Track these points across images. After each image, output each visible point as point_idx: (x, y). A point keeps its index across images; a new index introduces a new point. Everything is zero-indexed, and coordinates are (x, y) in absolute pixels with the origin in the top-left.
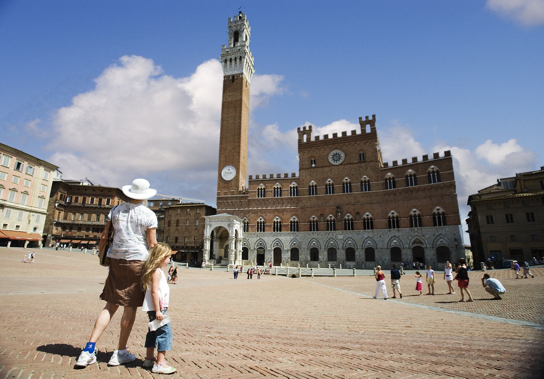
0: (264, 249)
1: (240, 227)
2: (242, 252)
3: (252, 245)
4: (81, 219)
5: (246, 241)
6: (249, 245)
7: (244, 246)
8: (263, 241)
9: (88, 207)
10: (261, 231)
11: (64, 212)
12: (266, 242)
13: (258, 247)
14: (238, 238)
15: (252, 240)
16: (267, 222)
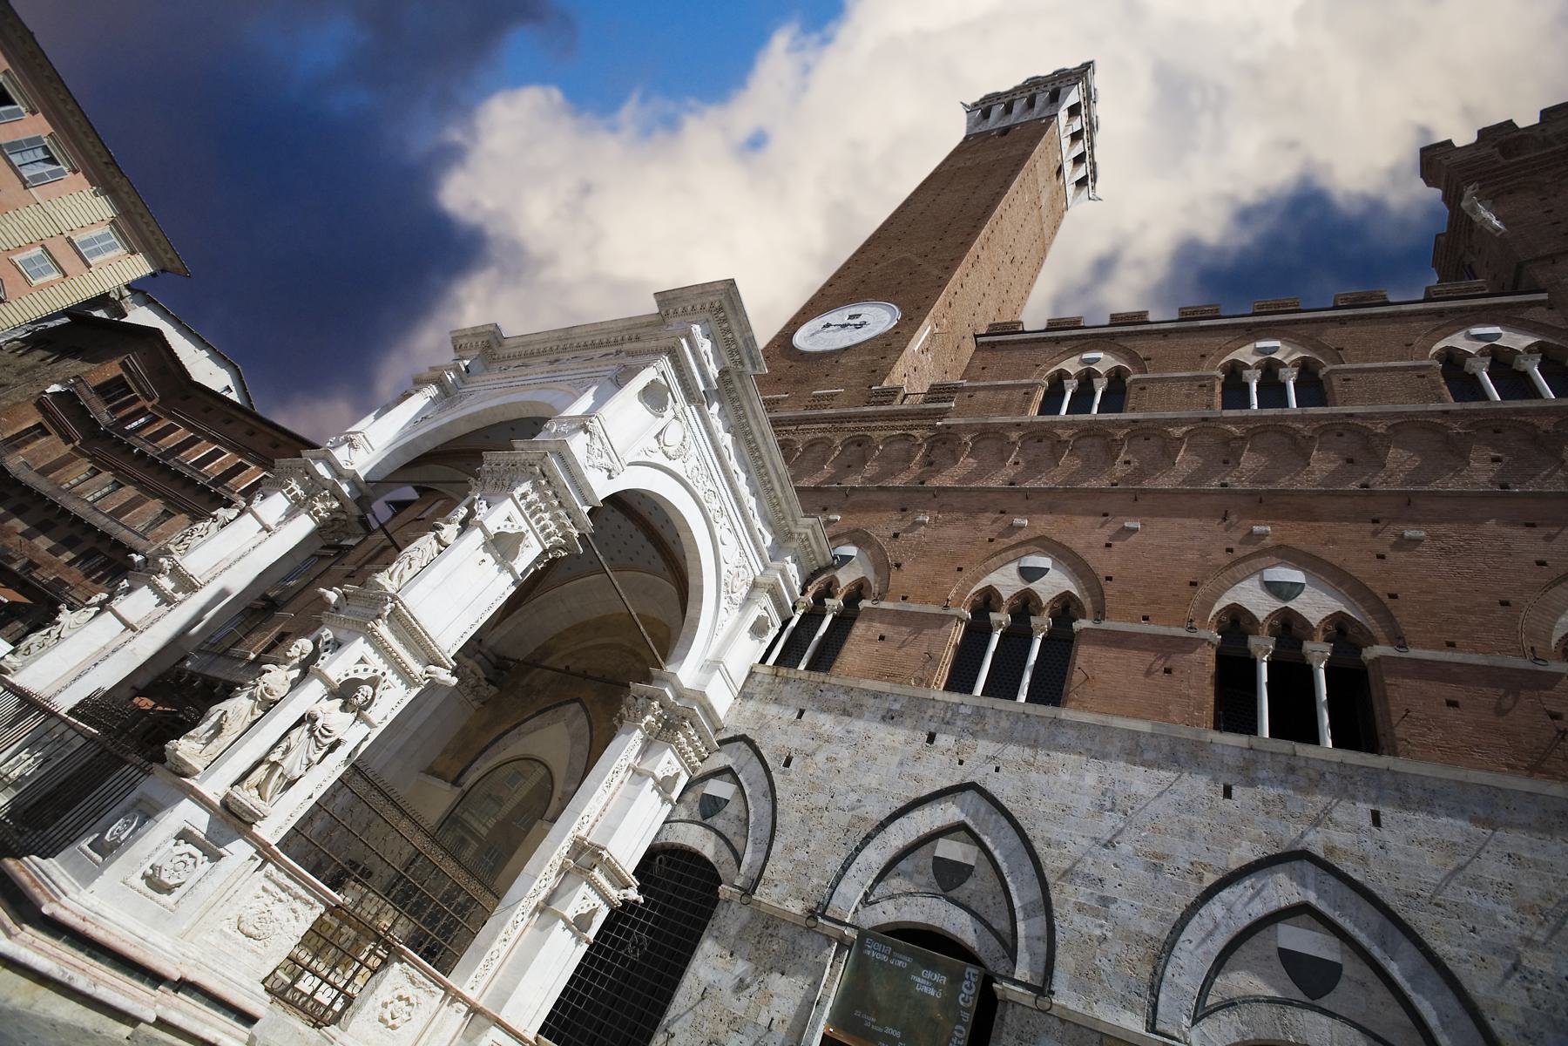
0: (987, 980)
1: (755, 585)
2: (620, 915)
3: (800, 854)
4: (95, 501)
5: (750, 773)
6: (758, 831)
7: (695, 838)
8: (1000, 844)
9: (179, 475)
10: (1002, 686)
11: (74, 449)
12: (1052, 862)
13: (886, 913)
14: (671, 680)
15: (839, 785)
16: (1108, 605)
